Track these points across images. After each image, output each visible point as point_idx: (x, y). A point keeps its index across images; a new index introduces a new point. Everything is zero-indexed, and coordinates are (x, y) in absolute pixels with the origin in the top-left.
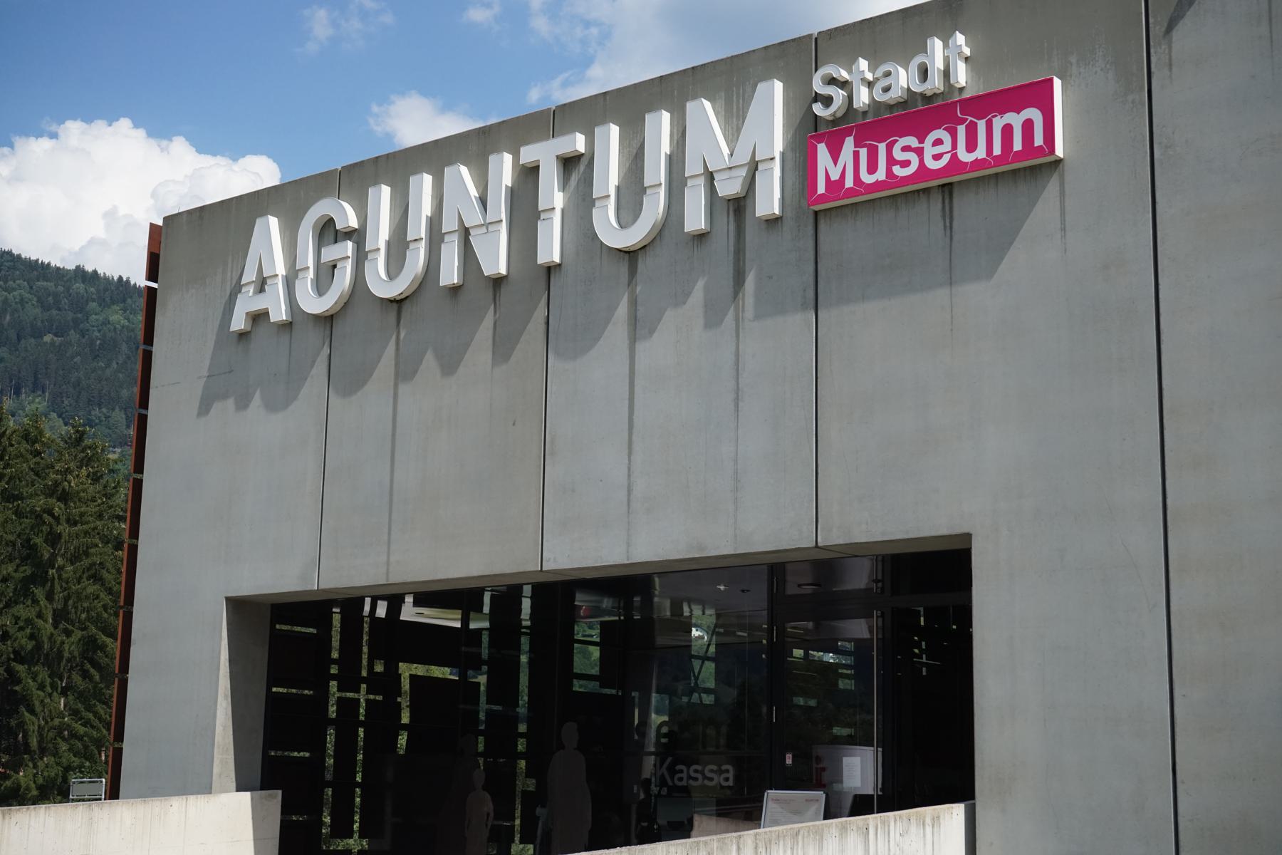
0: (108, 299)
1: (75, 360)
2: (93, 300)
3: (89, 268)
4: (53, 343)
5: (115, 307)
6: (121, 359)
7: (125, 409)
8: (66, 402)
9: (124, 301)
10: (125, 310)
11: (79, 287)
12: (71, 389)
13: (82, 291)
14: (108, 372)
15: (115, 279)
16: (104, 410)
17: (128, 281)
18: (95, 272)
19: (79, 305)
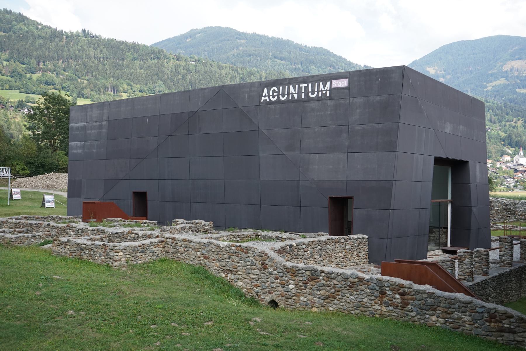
0: (18, 21)
1: (15, 42)
2: (14, 21)
3: (8, 10)
4: (5, 36)
5: (21, 23)
6: (30, 41)
7: (35, 59)
8: (15, 56)
9: (24, 21)
10: (25, 25)
11: (7, 16)
12: (16, 52)
13: (9, 18)
14: (27, 46)
15: (18, 13)
16: (28, 59)
17: (22, 15)
18: (11, 11)
19: (9, 22)
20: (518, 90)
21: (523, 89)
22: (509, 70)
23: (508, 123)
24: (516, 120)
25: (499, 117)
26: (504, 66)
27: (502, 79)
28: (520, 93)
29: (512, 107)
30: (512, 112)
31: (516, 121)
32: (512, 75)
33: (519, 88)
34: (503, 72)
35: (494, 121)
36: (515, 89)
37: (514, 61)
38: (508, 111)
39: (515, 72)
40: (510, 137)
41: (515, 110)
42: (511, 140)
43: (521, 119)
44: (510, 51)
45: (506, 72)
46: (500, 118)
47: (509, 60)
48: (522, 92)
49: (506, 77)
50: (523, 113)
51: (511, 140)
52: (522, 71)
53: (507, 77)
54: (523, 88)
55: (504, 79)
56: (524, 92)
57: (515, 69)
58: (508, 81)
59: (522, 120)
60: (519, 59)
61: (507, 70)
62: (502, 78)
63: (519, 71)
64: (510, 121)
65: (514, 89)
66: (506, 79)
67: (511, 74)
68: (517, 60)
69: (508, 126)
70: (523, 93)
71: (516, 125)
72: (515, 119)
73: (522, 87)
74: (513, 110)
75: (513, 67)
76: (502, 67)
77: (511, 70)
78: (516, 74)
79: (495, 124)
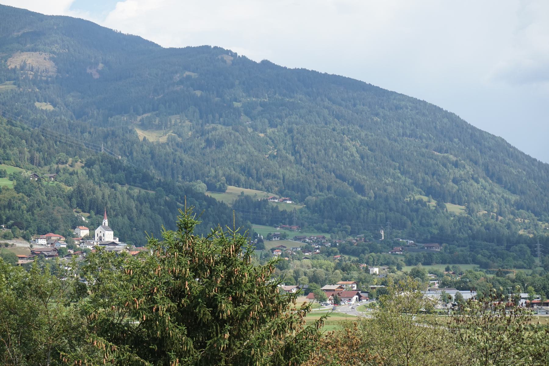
20: (37, 104)
21: (44, 103)
22: (18, 67)
23: (61, 166)
24: (73, 161)
25: (44, 155)
26: (10, 59)
27: (8, 82)
28: (42, 109)
29: (56, 137)
30: (56, 145)
31: (72, 164)
32: (24, 76)
33: (38, 101)
34: (8, 69)
35: (38, 161)
36: (32, 102)
37: (25, 53)
38: (51, 145)
39: (29, 72)
40: (79, 192)
41: (60, 142)
42: (81, 198)
43: (80, 160)
44: (15, 34)
45: (14, 70)
46: (46, 156)
47: (18, 50)
48: (44, 108)
49: (14, 79)
50: (74, 148)
51: (81, 198)
52: (40, 71)
53: (16, 79)
54: (45, 102)
55: (12, 82)
56: (48, 109)
57: (27, 67)
58: (19, 86)
59: (81, 162)
60: (34, 50)
61: (16, 66)
62: (7, 80)
63: (35, 70)
64: (63, 163)
65: (30, 101)
66: (15, 84)
67: (22, 74)
68: (29, 51)
69: (62, 171)
70: (46, 111)
71: (76, 171)
72: (70, 160)
73: (43, 101)
74: (58, 143)
75: (25, 62)
76: (6, 61)
77: (22, 68)
78: (31, 77)
79: (40, 168)
